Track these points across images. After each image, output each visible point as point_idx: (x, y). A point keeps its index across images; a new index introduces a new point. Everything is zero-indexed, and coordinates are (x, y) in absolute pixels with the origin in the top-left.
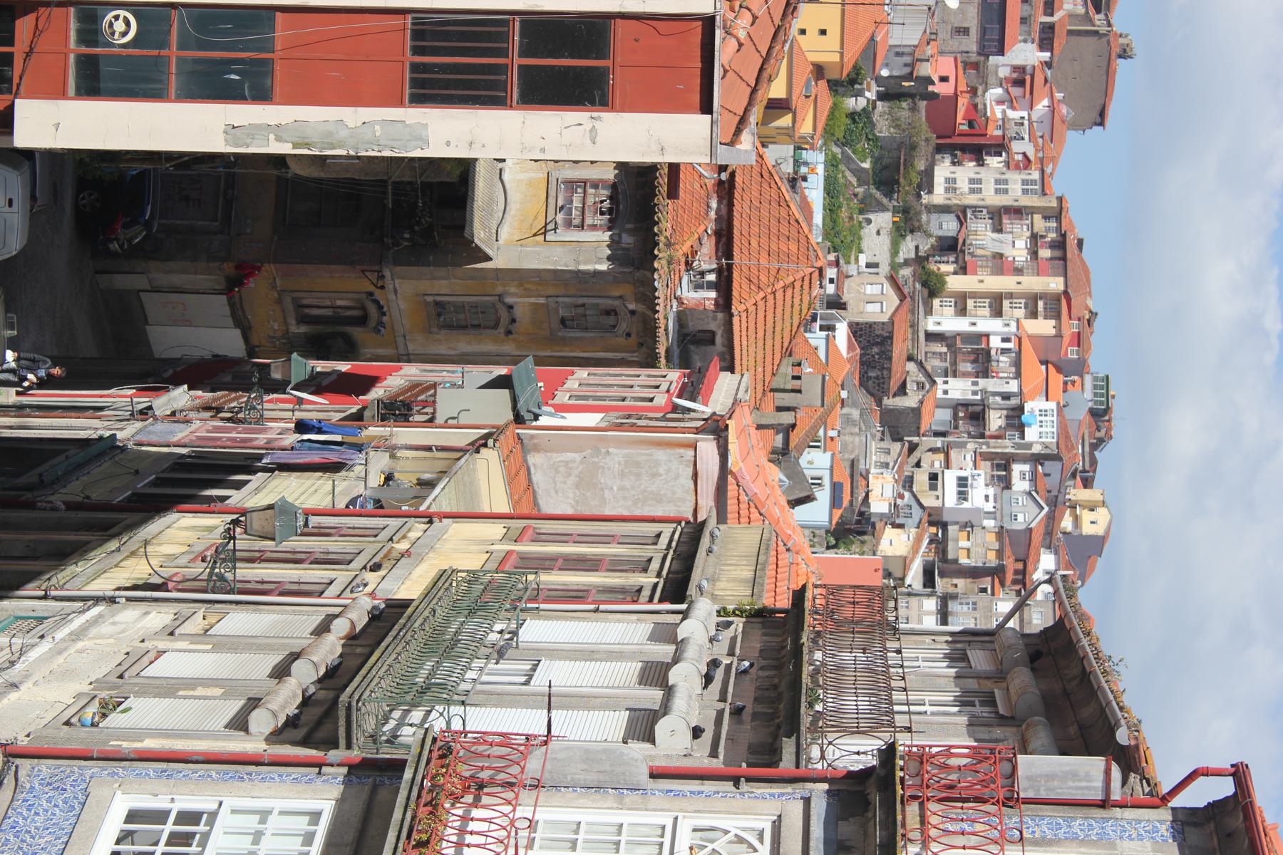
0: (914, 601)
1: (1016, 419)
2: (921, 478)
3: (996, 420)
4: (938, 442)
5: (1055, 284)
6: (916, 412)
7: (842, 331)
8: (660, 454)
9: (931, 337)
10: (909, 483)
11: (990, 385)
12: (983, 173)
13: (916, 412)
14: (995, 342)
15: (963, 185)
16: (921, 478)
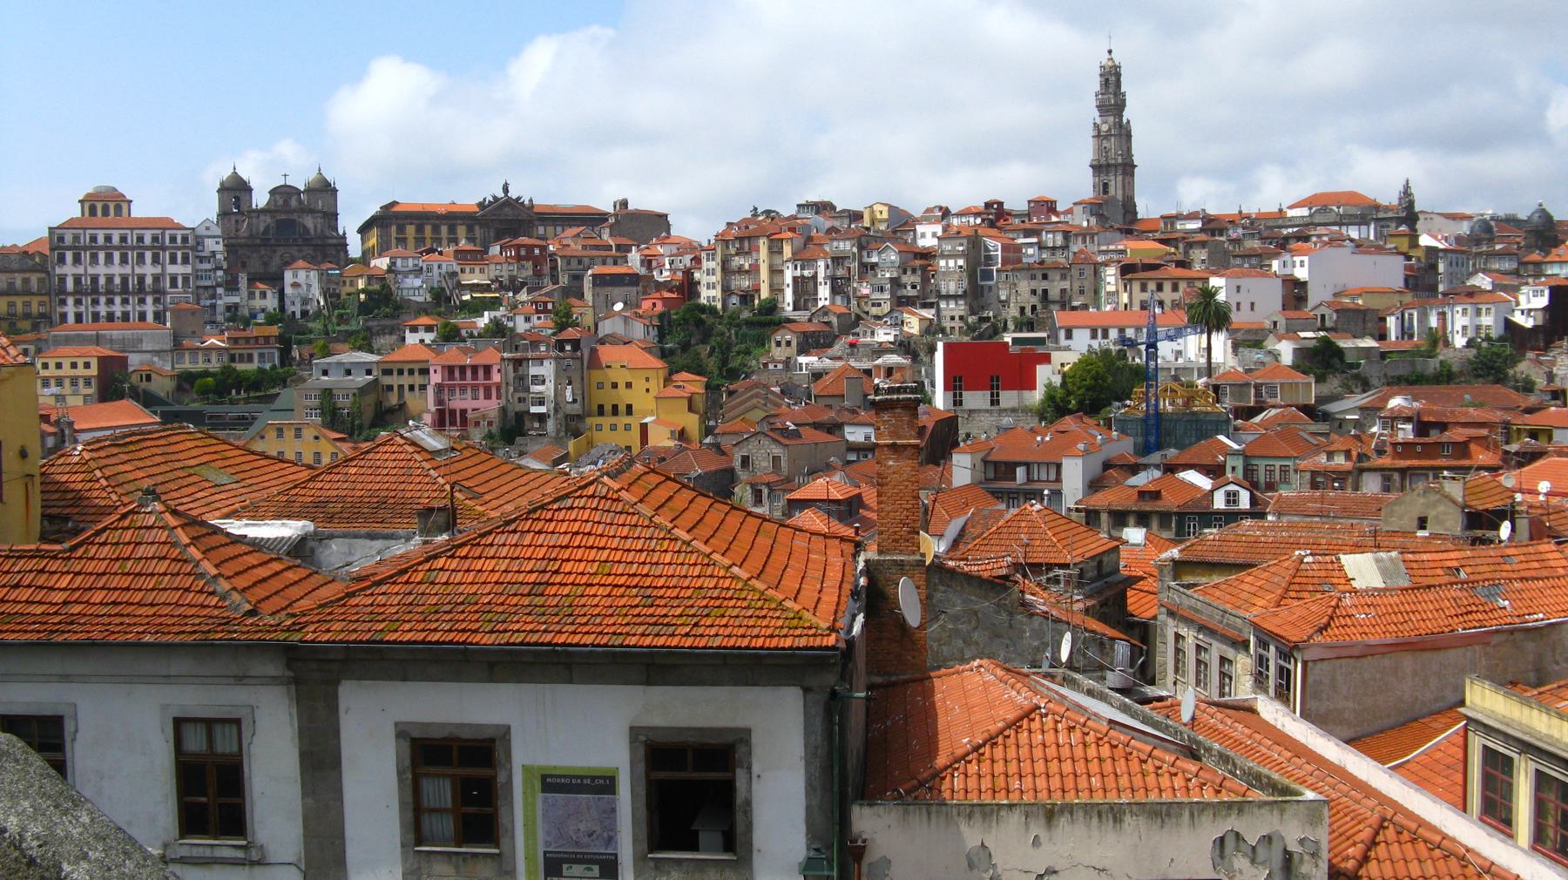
0: (944, 313)
1: (838, 260)
2: (874, 311)
3: (840, 272)
4: (854, 302)
5: (763, 245)
6: (839, 316)
7: (802, 360)
8: (1310, 680)
9: (795, 309)
10: (878, 318)
11: (820, 278)
12: (704, 282)
13: (839, 316)
14: (798, 273)
15: (712, 293)
16: (874, 311)
